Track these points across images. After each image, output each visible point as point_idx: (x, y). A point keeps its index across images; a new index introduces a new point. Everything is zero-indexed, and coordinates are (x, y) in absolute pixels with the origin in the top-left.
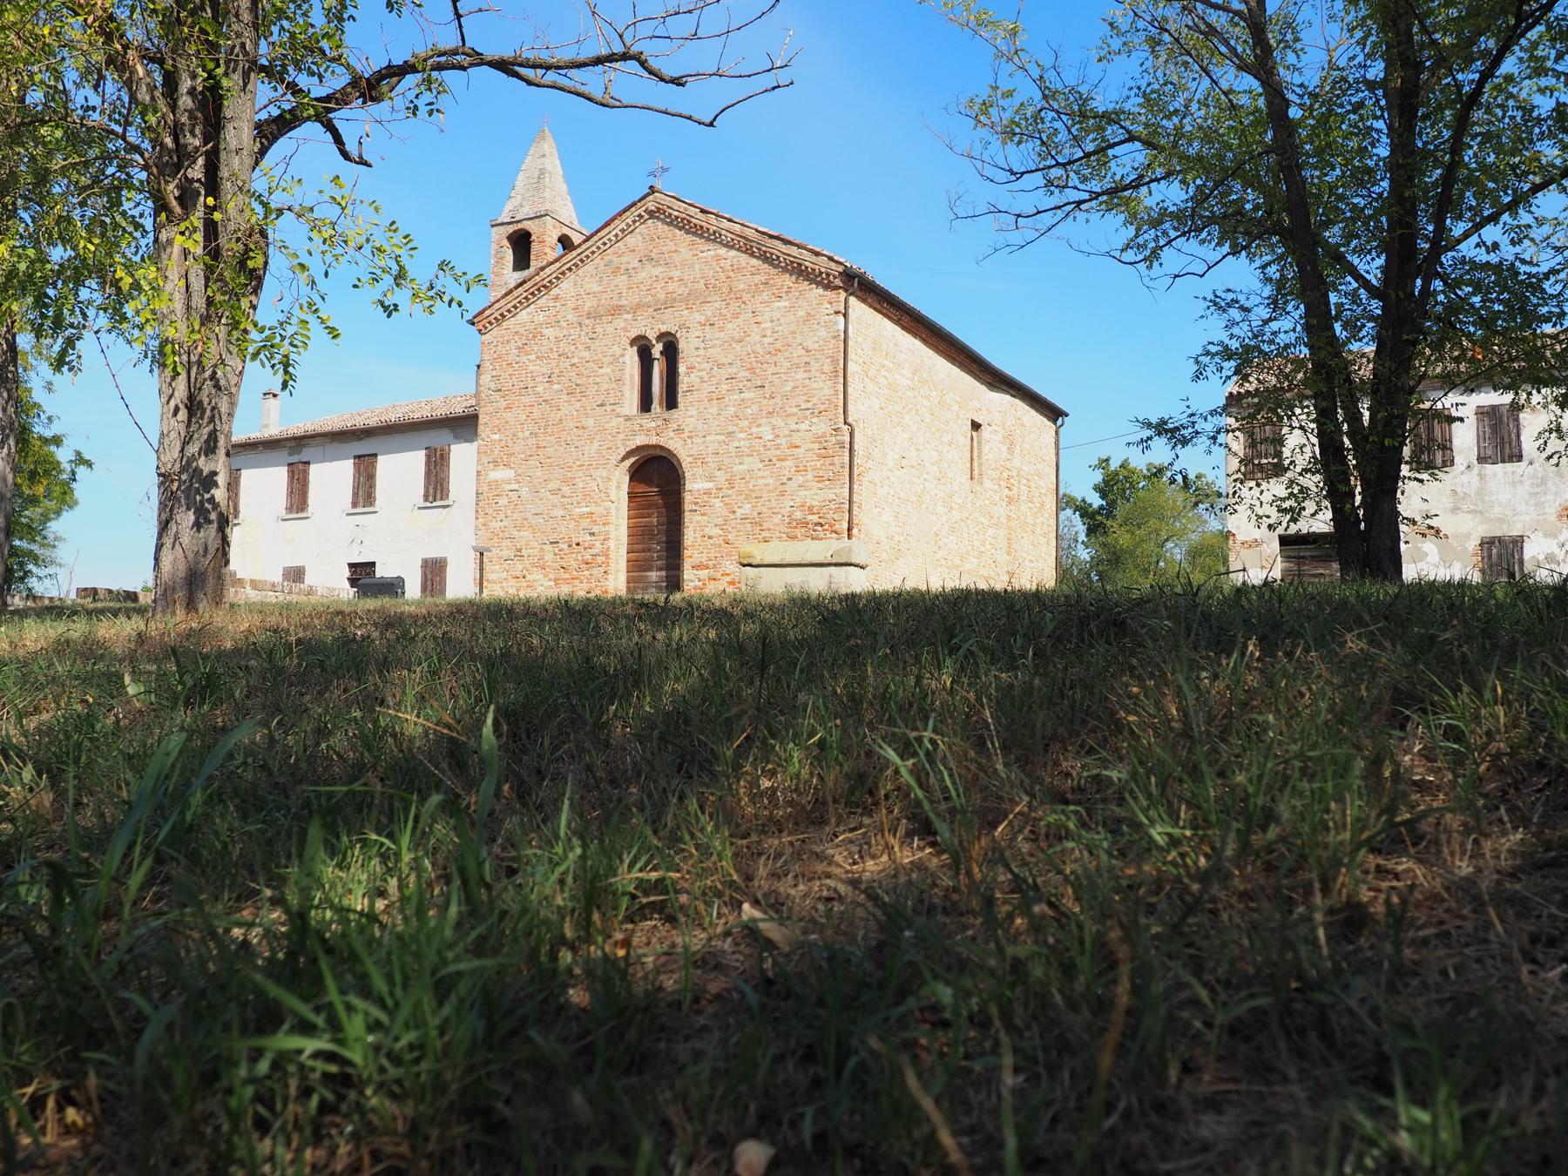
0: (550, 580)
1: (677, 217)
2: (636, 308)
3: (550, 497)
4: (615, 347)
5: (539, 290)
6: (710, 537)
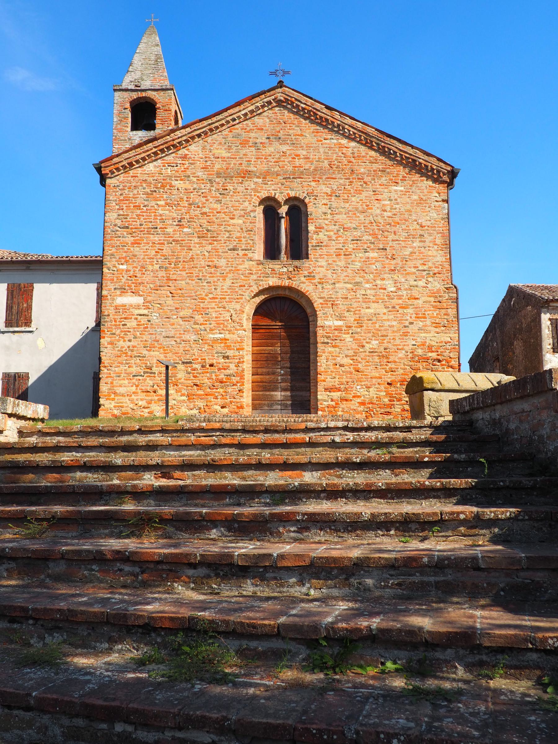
0: (183, 395)
1: (304, 109)
2: (265, 175)
3: (182, 323)
4: (247, 204)
5: (167, 148)
6: (341, 366)
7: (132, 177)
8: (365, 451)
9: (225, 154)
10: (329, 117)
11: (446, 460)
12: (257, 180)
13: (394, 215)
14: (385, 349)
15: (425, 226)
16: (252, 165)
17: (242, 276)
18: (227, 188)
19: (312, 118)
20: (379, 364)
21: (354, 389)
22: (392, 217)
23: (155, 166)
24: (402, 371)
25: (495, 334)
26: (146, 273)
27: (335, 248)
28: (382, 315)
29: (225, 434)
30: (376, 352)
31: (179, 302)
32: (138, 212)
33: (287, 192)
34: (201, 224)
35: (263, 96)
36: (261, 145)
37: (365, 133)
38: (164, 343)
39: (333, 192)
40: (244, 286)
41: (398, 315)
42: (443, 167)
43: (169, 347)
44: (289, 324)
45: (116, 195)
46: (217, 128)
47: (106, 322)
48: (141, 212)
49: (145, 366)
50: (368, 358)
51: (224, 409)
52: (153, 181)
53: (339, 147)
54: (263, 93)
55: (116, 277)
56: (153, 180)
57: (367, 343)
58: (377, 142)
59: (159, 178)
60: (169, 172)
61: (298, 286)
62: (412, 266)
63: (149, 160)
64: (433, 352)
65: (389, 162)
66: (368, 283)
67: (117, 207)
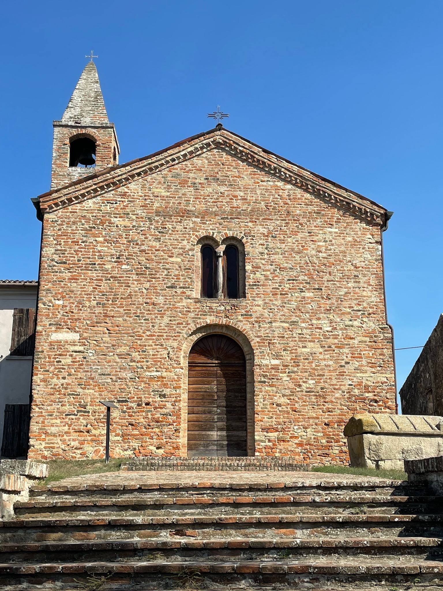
1: (241, 152)
2: (204, 215)
3: (118, 360)
6: (278, 405)
7: (71, 212)
8: (341, 510)
9: (164, 193)
10: (266, 160)
11: (414, 521)
12: (196, 219)
13: (329, 255)
14: (322, 389)
15: (359, 267)
16: (190, 205)
17: (180, 314)
18: (166, 226)
19: (250, 160)
20: (316, 404)
21: (292, 429)
22: (327, 258)
23: (94, 203)
24: (339, 411)
25: (427, 364)
26: (82, 309)
27: (271, 287)
28: (318, 355)
29: (214, 492)
30: (313, 392)
31: (116, 339)
32: (77, 247)
33: (225, 232)
34: (140, 262)
35: (202, 138)
36: (200, 186)
37: (301, 177)
38: (100, 381)
39: (270, 232)
40: (182, 324)
41: (334, 355)
42: (376, 210)
43: (104, 385)
44: (226, 362)
45: (54, 230)
46: (157, 167)
47: (40, 358)
48: (79, 248)
49: (79, 405)
50: (305, 397)
51: (160, 450)
52: (92, 218)
53: (276, 189)
54: (203, 135)
55: (52, 313)
56: (92, 216)
57: (304, 382)
58: (313, 185)
59: (98, 215)
60: (108, 209)
61: (236, 325)
62: (347, 306)
63: (88, 197)
64: (369, 392)
65: (323, 205)
66: (304, 322)
67: (55, 242)
